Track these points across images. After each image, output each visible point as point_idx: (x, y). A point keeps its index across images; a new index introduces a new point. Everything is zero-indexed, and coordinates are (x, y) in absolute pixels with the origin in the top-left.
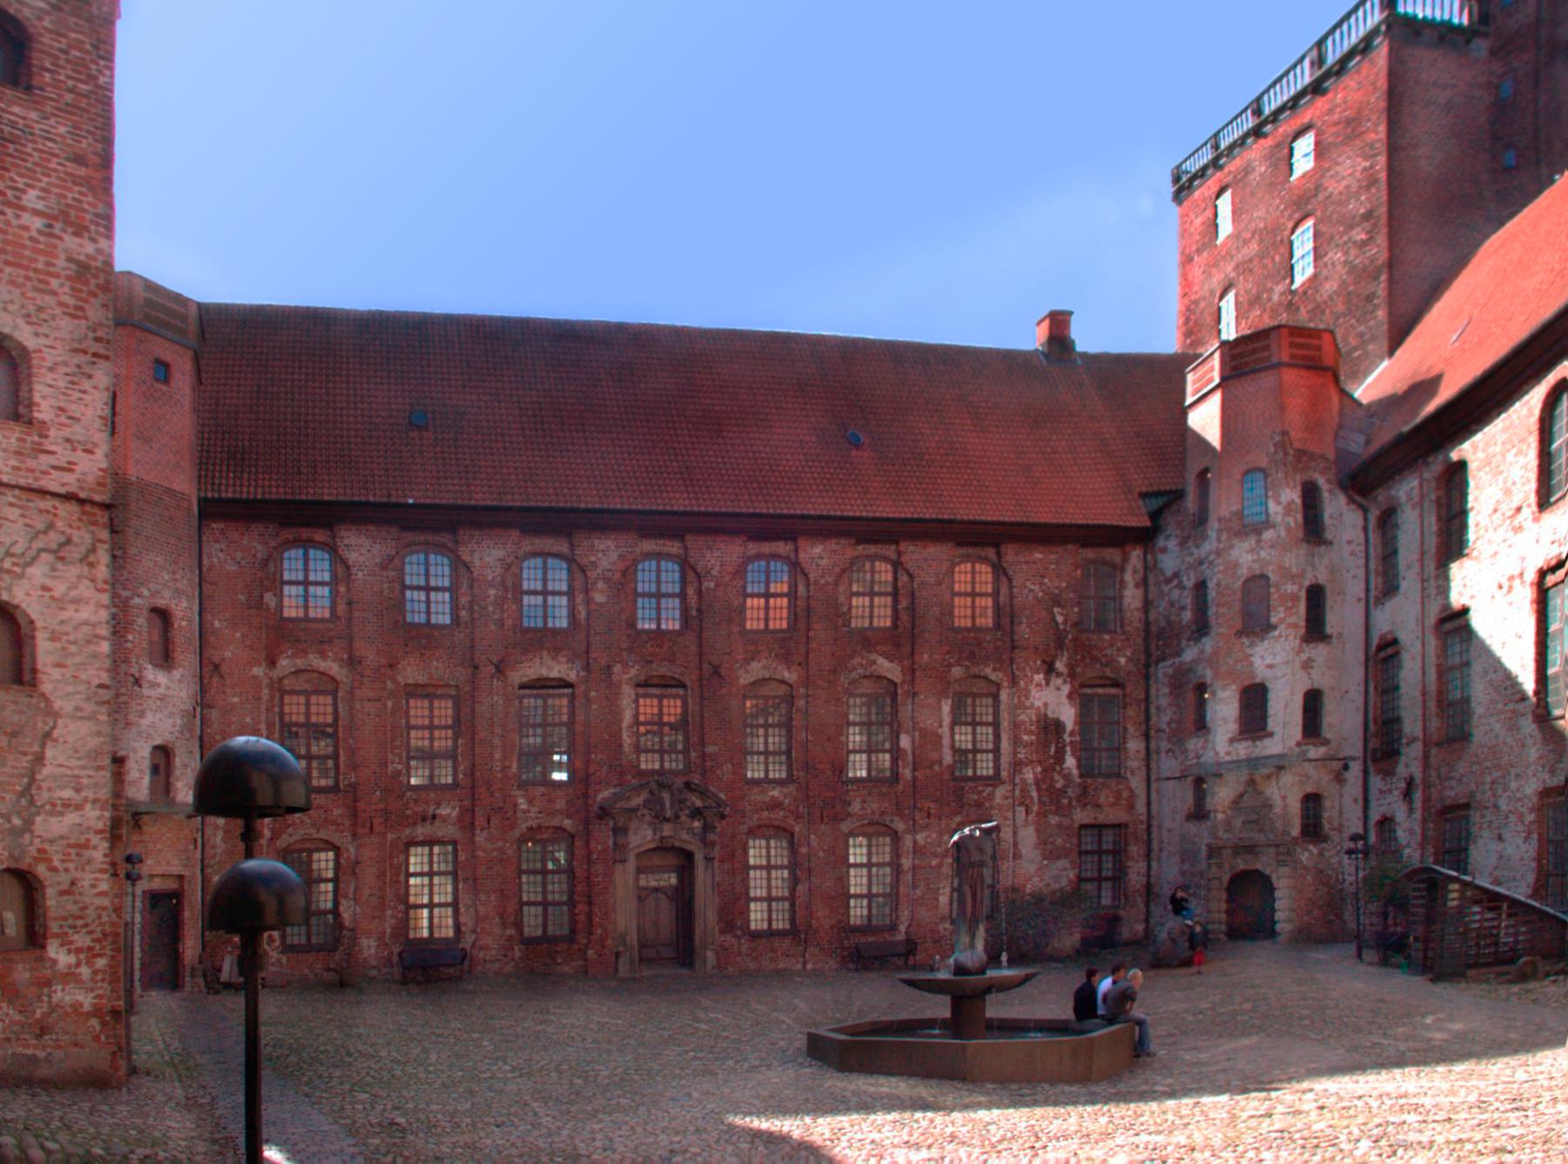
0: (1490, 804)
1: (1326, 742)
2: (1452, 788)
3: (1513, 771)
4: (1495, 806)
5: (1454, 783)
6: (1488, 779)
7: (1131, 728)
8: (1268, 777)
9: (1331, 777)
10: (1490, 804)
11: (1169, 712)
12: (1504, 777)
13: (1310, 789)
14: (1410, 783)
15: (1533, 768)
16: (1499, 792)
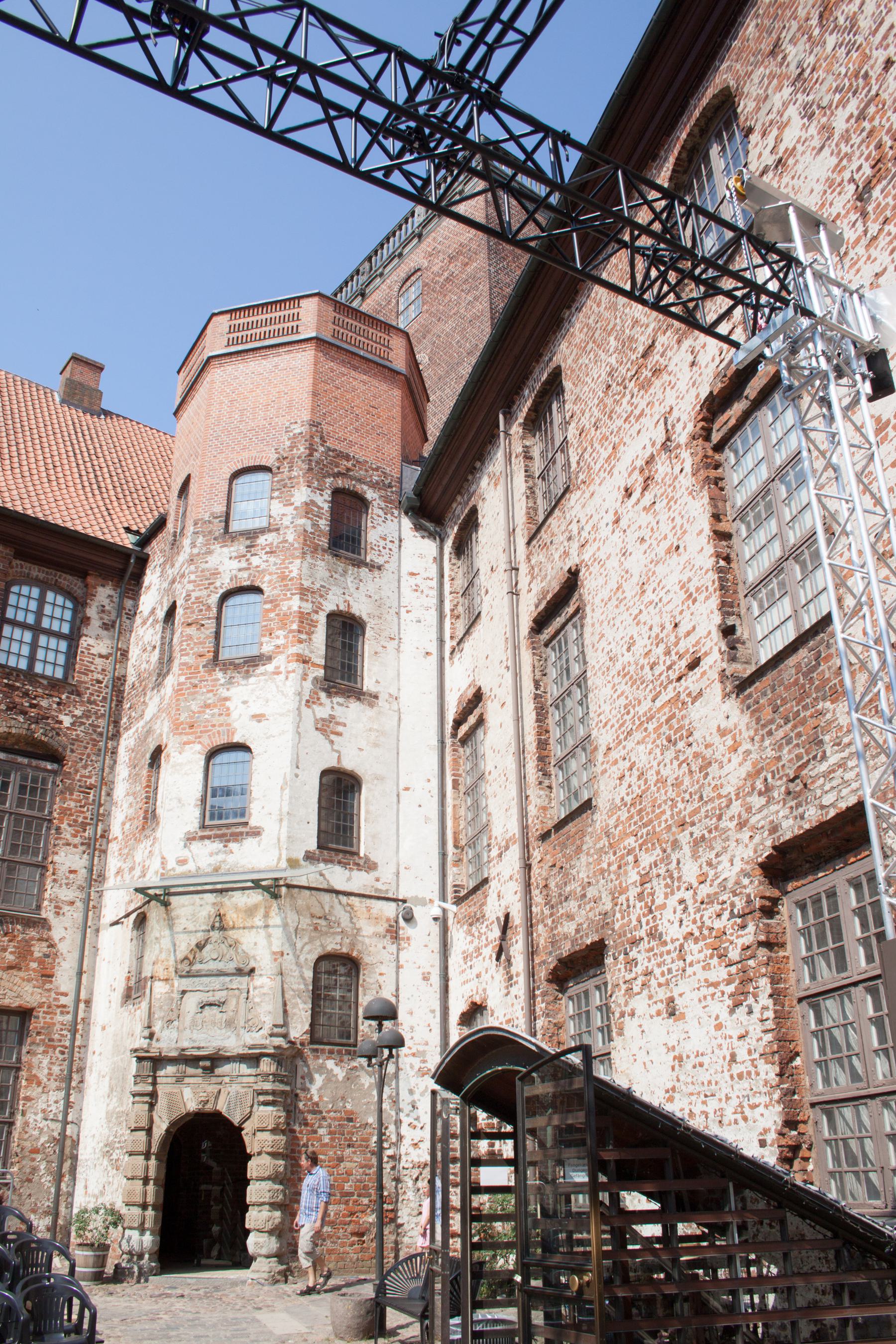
0: (642, 933)
1: (370, 866)
2: (570, 917)
3: (684, 838)
4: (654, 934)
5: (572, 905)
6: (633, 876)
7: (67, 832)
8: (250, 911)
9: (382, 928)
10: (642, 933)
11: (125, 806)
12: (666, 859)
13: (332, 945)
14: (506, 925)
15: (736, 807)
16: (659, 901)
